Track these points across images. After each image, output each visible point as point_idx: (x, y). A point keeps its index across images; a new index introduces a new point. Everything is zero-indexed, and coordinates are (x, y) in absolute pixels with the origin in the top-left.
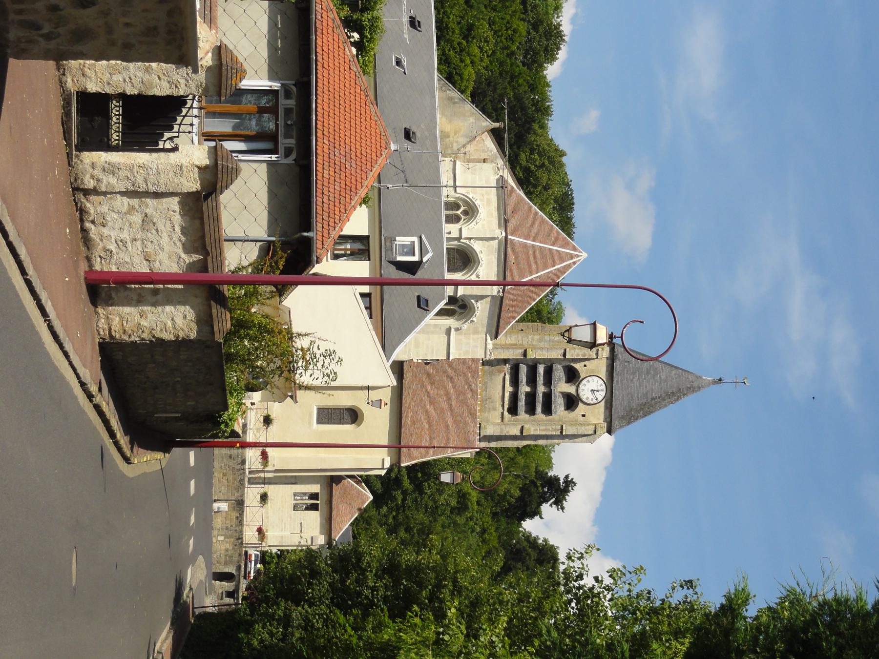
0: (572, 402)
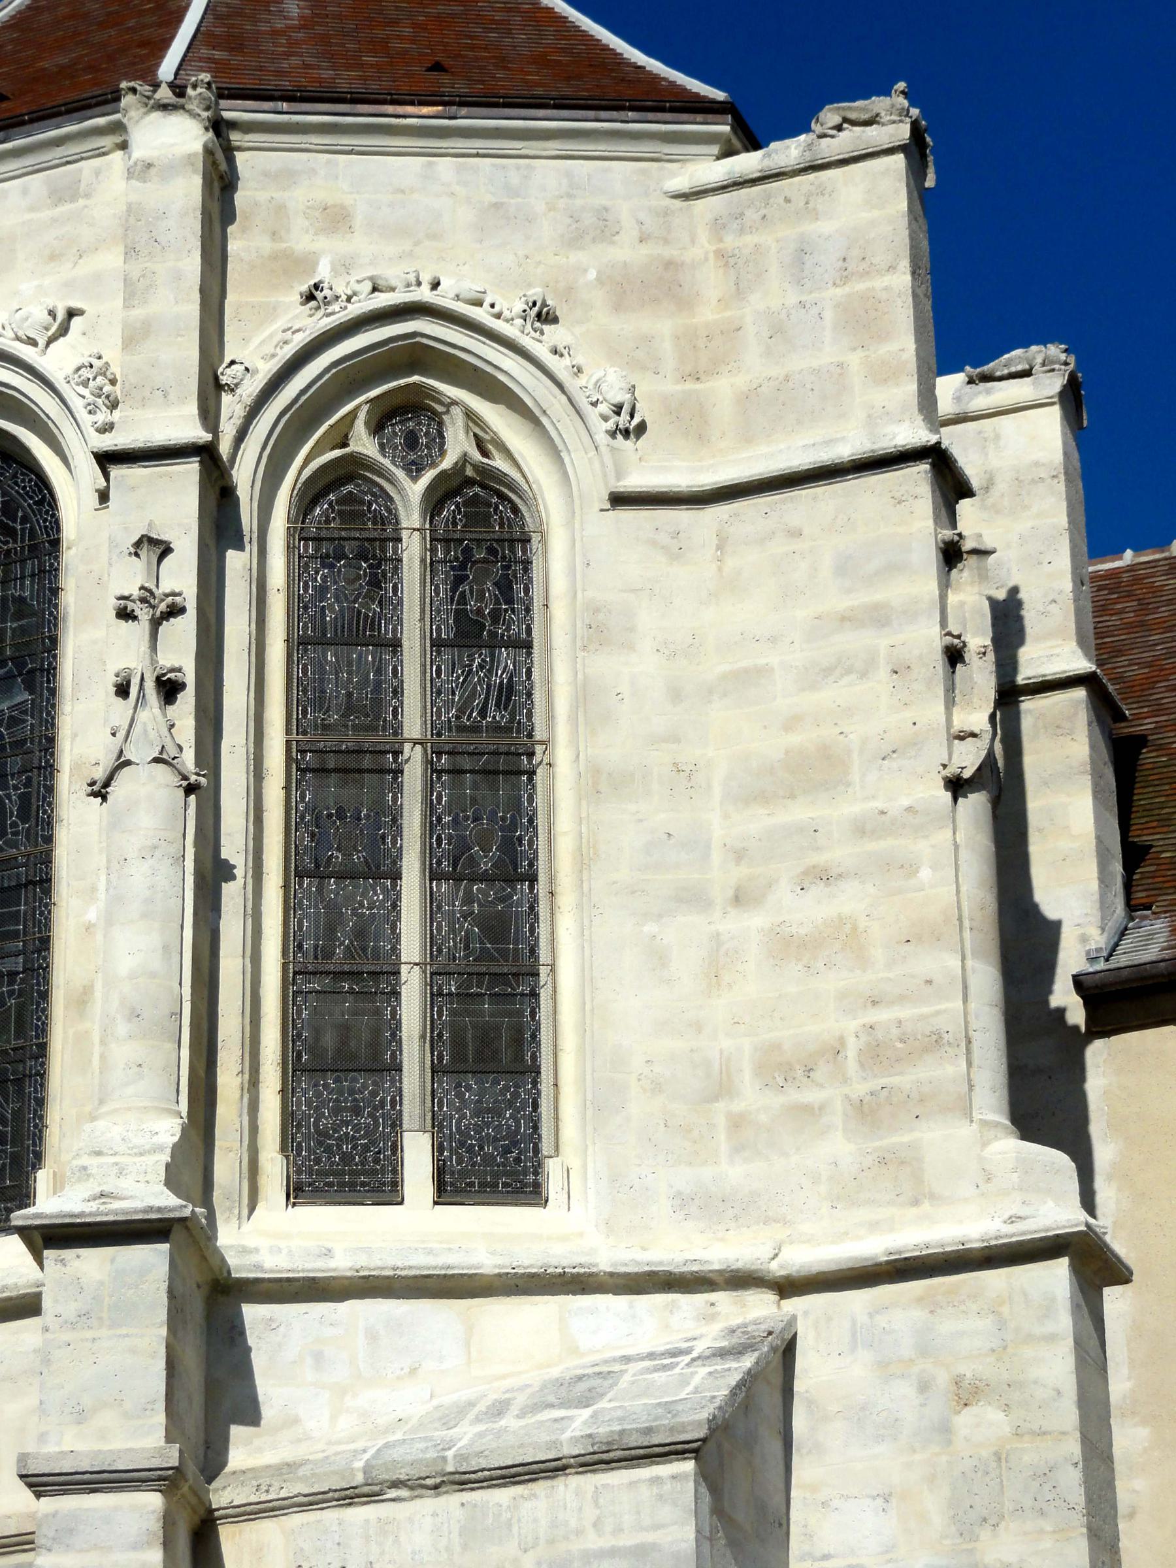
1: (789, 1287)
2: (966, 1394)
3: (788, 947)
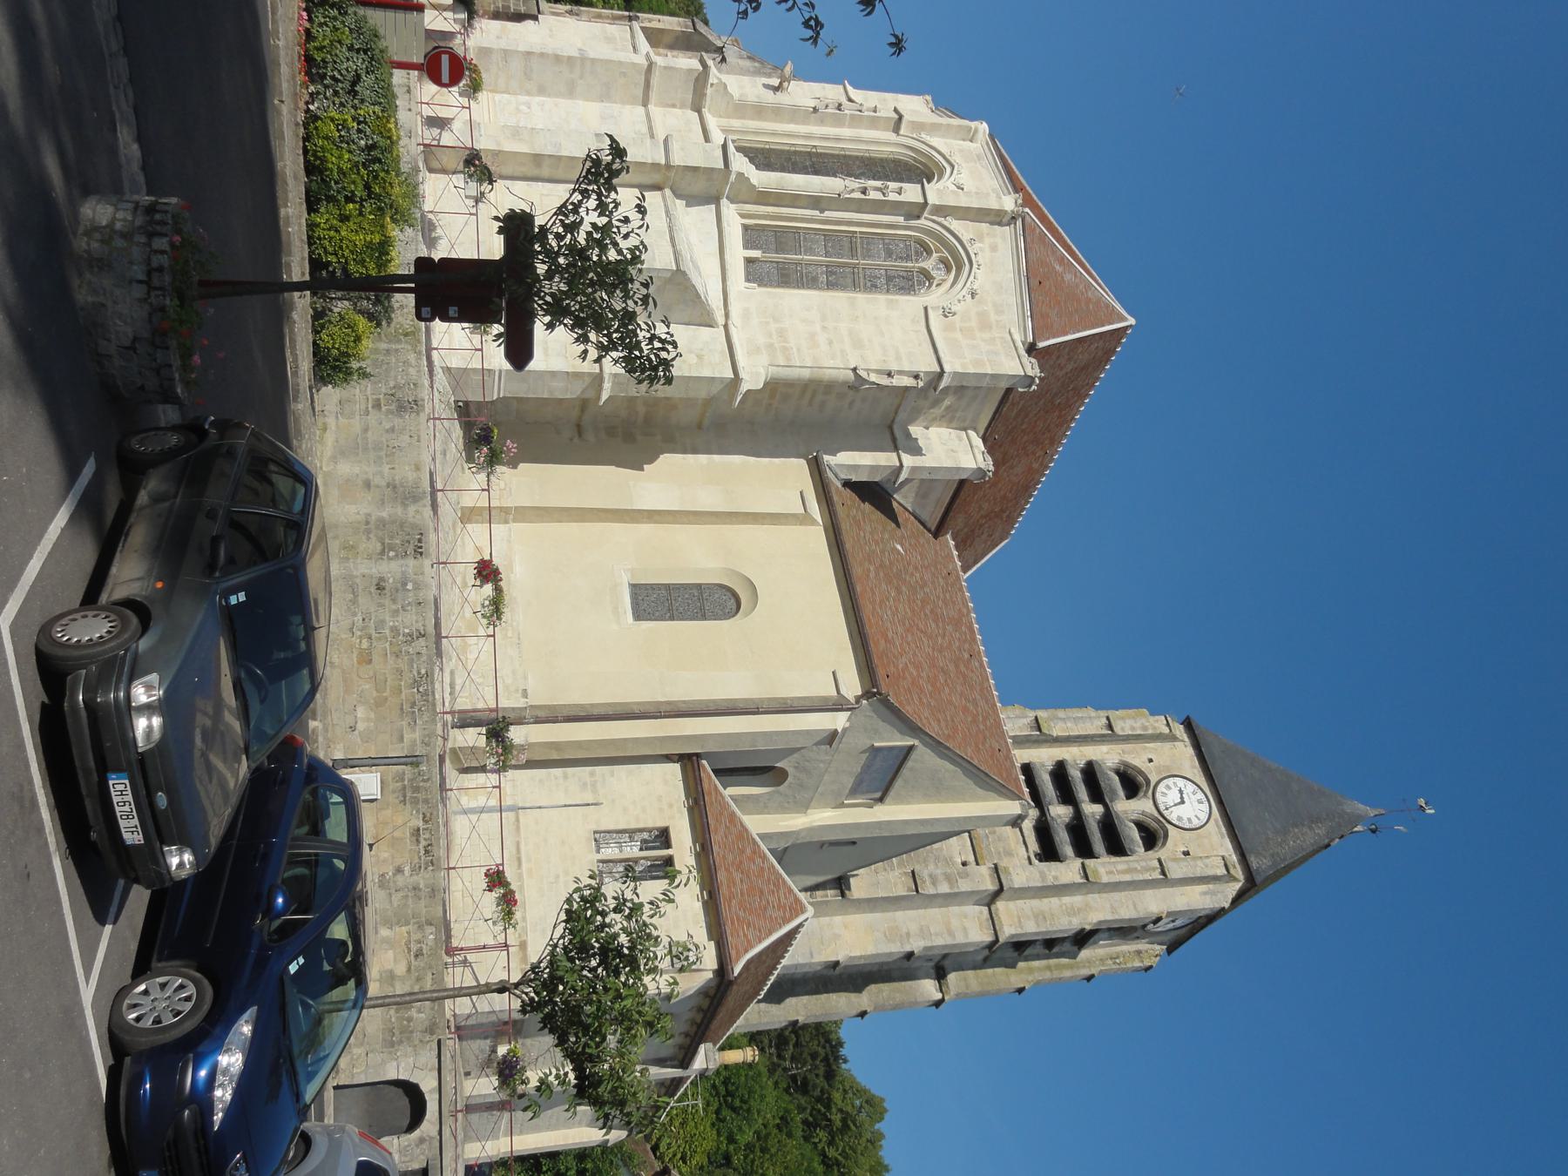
0: (1152, 837)
1: (726, 326)
2: (700, 357)
3: (812, 336)
